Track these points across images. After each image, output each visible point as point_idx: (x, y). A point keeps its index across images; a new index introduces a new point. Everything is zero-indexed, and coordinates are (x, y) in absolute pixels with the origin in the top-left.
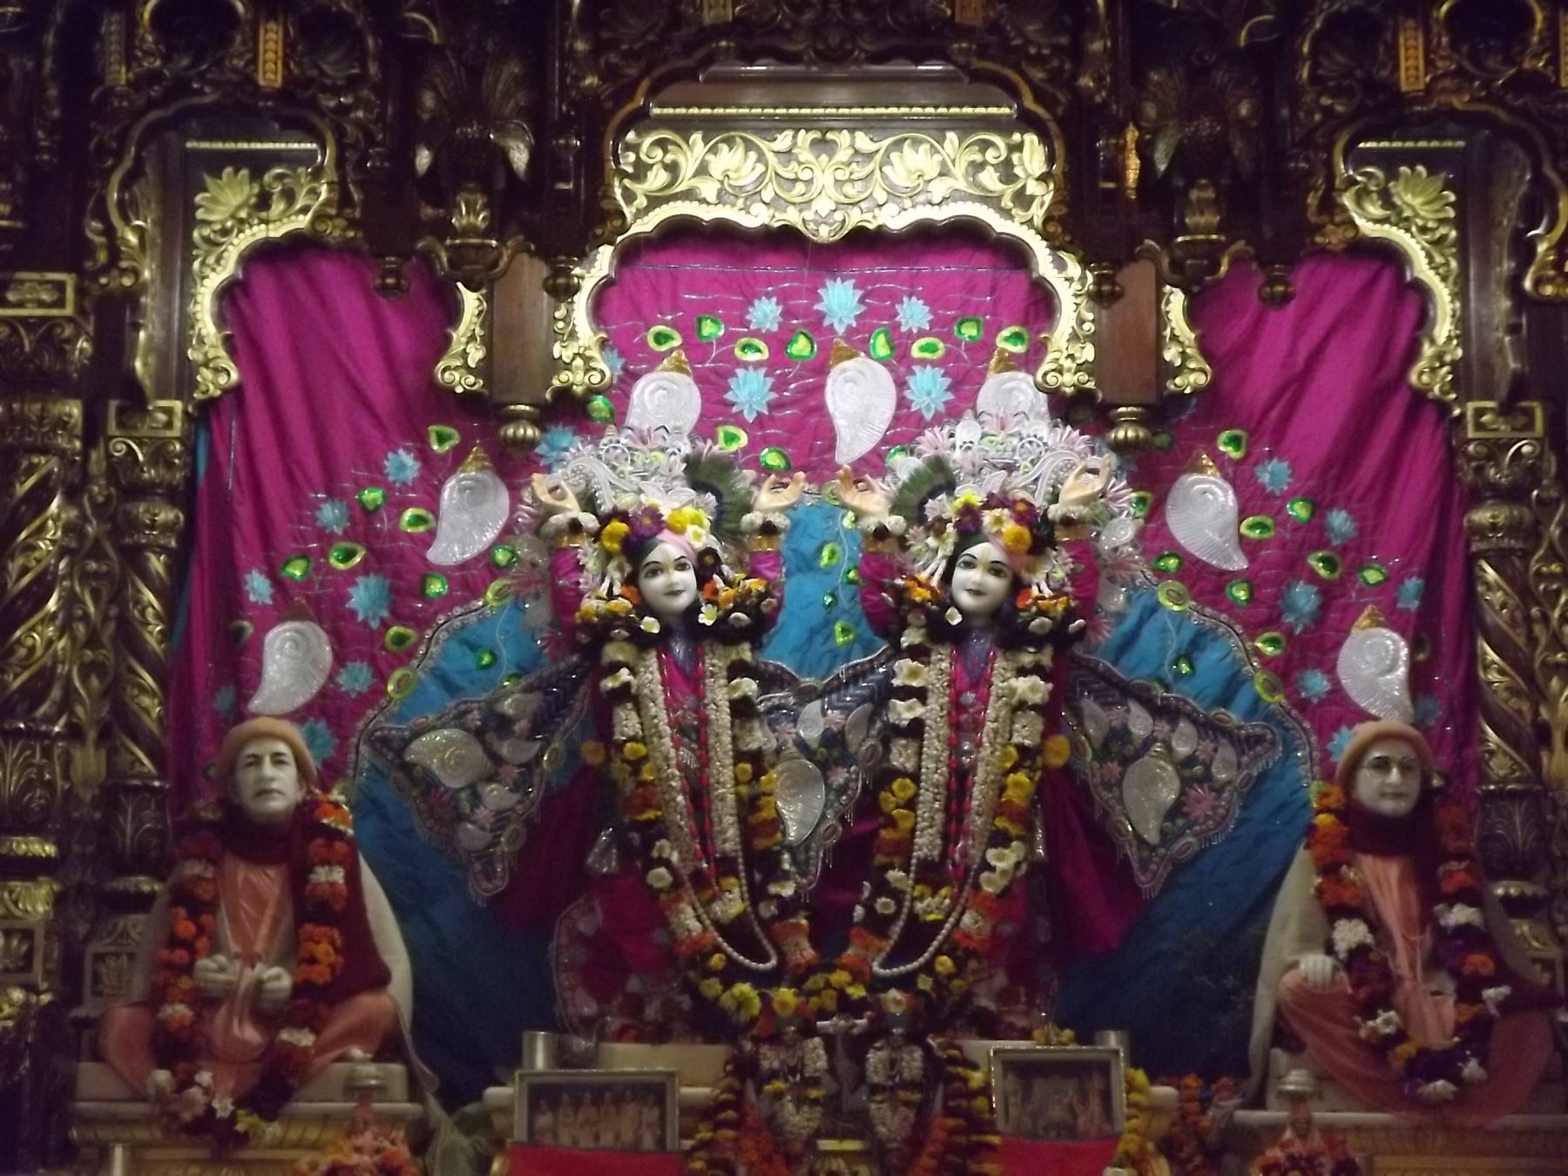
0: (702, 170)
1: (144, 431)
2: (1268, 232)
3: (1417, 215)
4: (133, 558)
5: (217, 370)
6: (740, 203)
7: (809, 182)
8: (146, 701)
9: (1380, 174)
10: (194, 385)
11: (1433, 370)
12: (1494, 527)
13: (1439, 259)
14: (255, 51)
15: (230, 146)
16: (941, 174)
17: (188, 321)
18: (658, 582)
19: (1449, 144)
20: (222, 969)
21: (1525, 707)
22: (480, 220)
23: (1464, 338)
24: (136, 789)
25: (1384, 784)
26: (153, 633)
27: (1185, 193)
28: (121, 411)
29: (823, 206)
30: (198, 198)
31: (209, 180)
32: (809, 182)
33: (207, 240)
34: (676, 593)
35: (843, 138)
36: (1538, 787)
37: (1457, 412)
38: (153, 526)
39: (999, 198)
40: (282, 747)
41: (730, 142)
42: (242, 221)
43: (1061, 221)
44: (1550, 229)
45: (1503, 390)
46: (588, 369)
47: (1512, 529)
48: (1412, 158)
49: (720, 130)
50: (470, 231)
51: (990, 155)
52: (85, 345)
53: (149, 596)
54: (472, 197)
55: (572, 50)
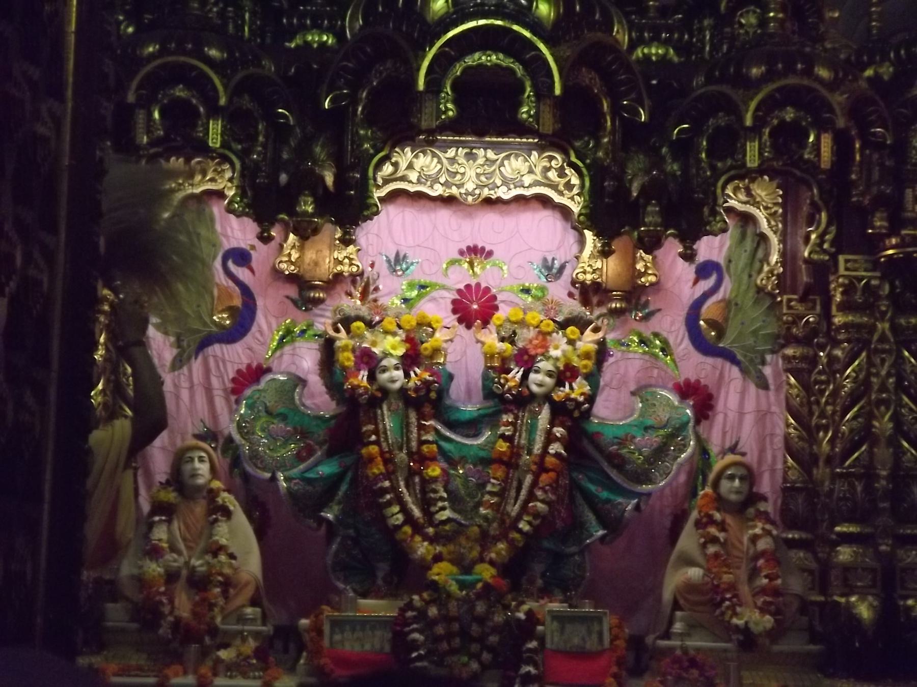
0: (410, 166)
2: (684, 226)
3: (763, 201)
6: (429, 183)
7: (463, 174)
12: (794, 357)
13: (773, 223)
16: (529, 172)
18: (385, 376)
20: (175, 561)
22: (310, 209)
23: (784, 264)
25: (732, 487)
27: (645, 207)
29: (470, 186)
32: (463, 174)
35: (481, 152)
36: (810, 486)
37: (779, 299)
39: (558, 185)
40: (203, 454)
41: (424, 153)
44: (817, 228)
45: (801, 289)
46: (351, 264)
47: (803, 358)
50: (305, 213)
51: (553, 163)
54: (306, 199)
55: (357, 132)
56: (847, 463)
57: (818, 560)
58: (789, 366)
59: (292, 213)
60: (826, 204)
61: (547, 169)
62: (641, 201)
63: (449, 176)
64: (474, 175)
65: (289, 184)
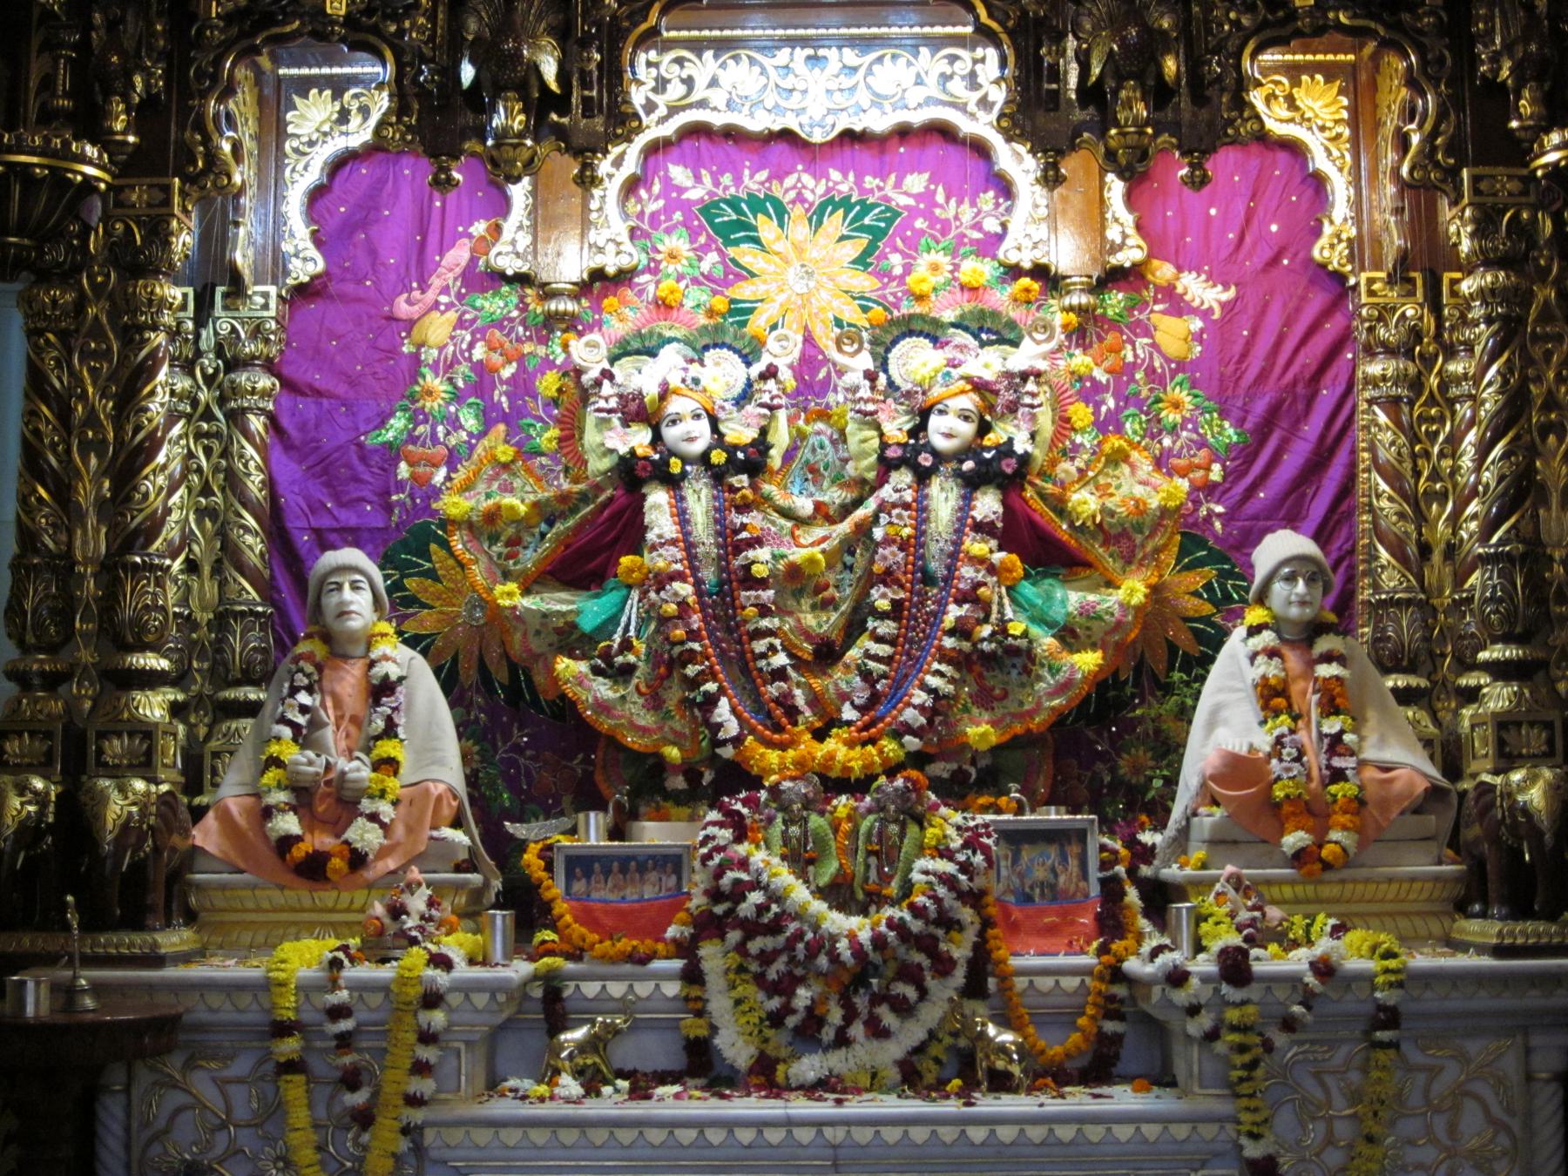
1: (244, 312)
4: (236, 418)
7: (805, 92)
8: (249, 539)
9: (1285, 80)
10: (286, 273)
11: (1332, 246)
12: (1384, 378)
13: (1336, 153)
15: (315, 71)
17: (279, 220)
19: (1341, 57)
20: (310, 763)
21: (1411, 528)
22: (518, 121)
23: (1358, 220)
24: (242, 613)
26: (255, 483)
27: (1115, 93)
28: (225, 296)
29: (816, 109)
30: (289, 116)
31: (297, 99)
32: (805, 92)
33: (296, 150)
34: (691, 440)
35: (831, 54)
37: (1352, 281)
38: (253, 392)
41: (736, 58)
42: (325, 134)
43: (1011, 116)
48: (1312, 69)
49: (730, 49)
51: (958, 64)
52: (188, 239)
53: (250, 450)
56: (1494, 539)
57: (1437, 721)
58: (1376, 393)
61: (946, 78)
62: (1110, 83)
65: (477, 81)
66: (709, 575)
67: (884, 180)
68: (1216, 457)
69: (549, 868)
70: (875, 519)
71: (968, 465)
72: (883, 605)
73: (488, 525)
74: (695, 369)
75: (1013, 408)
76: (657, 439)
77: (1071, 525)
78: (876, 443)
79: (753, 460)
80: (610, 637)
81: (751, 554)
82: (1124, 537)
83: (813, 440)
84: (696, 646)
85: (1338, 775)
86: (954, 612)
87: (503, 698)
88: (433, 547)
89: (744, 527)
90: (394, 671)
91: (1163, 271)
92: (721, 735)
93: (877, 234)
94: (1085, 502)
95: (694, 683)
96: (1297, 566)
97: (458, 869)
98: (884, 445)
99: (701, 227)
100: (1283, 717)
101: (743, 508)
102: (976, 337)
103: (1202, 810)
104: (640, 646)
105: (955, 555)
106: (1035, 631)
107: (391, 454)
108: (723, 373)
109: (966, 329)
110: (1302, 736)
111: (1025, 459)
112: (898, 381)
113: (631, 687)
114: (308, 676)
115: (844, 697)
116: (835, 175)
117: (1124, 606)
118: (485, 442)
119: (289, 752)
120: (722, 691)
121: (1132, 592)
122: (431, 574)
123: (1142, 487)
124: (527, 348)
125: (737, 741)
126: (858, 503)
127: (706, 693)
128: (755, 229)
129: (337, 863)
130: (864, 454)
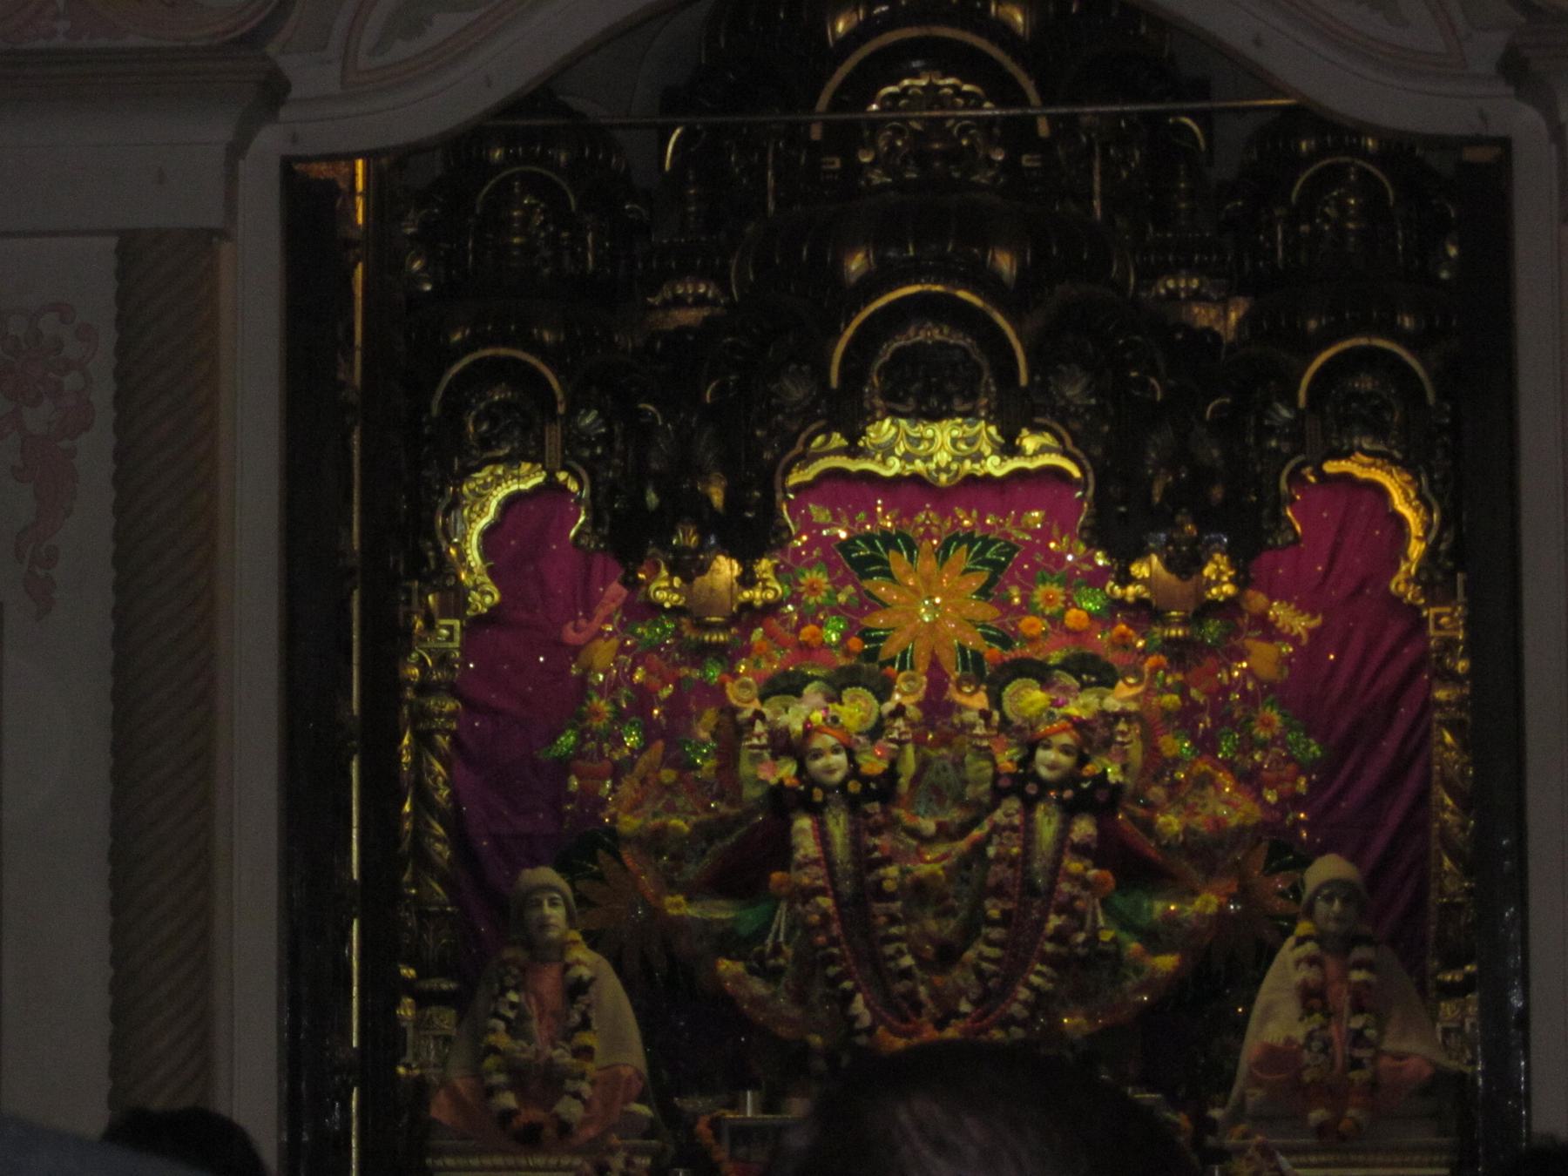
5: (483, 593)
7: (932, 440)
8: (439, 847)
10: (467, 605)
12: (1448, 703)
14: (543, 447)
18: (819, 764)
29: (943, 458)
32: (932, 440)
33: (472, 491)
38: (440, 715)
53: (438, 767)
55: (753, 435)
59: (665, 545)
60: (1439, 497)
63: (911, 444)
64: (948, 440)
66: (846, 887)
67: (1005, 515)
68: (1302, 770)
69: (717, 1136)
70: (987, 840)
71: (1068, 794)
72: (994, 913)
73: (654, 842)
74: (834, 708)
75: (1108, 743)
76: (802, 770)
77: (1158, 842)
78: (990, 772)
79: (885, 787)
80: (762, 942)
81: (882, 872)
82: (1207, 852)
83: (937, 765)
84: (836, 951)
85: (1357, 1064)
86: (1054, 921)
87: (669, 985)
88: (600, 852)
89: (876, 848)
90: (585, 973)
91: (1257, 600)
92: (857, 1026)
93: (997, 567)
94: (1170, 822)
95: (834, 982)
96: (1334, 888)
97: (645, 1136)
98: (997, 775)
99: (838, 562)
100: (1317, 1016)
101: (877, 831)
102: (1078, 677)
103: (1249, 1091)
104: (788, 951)
105: (1055, 869)
106: (1124, 936)
107: (563, 766)
108: (856, 709)
109: (1070, 671)
110: (1333, 1031)
111: (1118, 787)
112: (1011, 715)
113: (782, 987)
114: (515, 977)
115: (961, 992)
116: (960, 513)
117: (1200, 916)
118: (646, 757)
119: (502, 1040)
120: (857, 989)
121: (1207, 903)
122: (599, 877)
123: (1228, 806)
124: (684, 671)
125: (870, 1031)
126: (976, 822)
127: (844, 991)
128: (886, 563)
129: (549, 1131)
130: (978, 782)
